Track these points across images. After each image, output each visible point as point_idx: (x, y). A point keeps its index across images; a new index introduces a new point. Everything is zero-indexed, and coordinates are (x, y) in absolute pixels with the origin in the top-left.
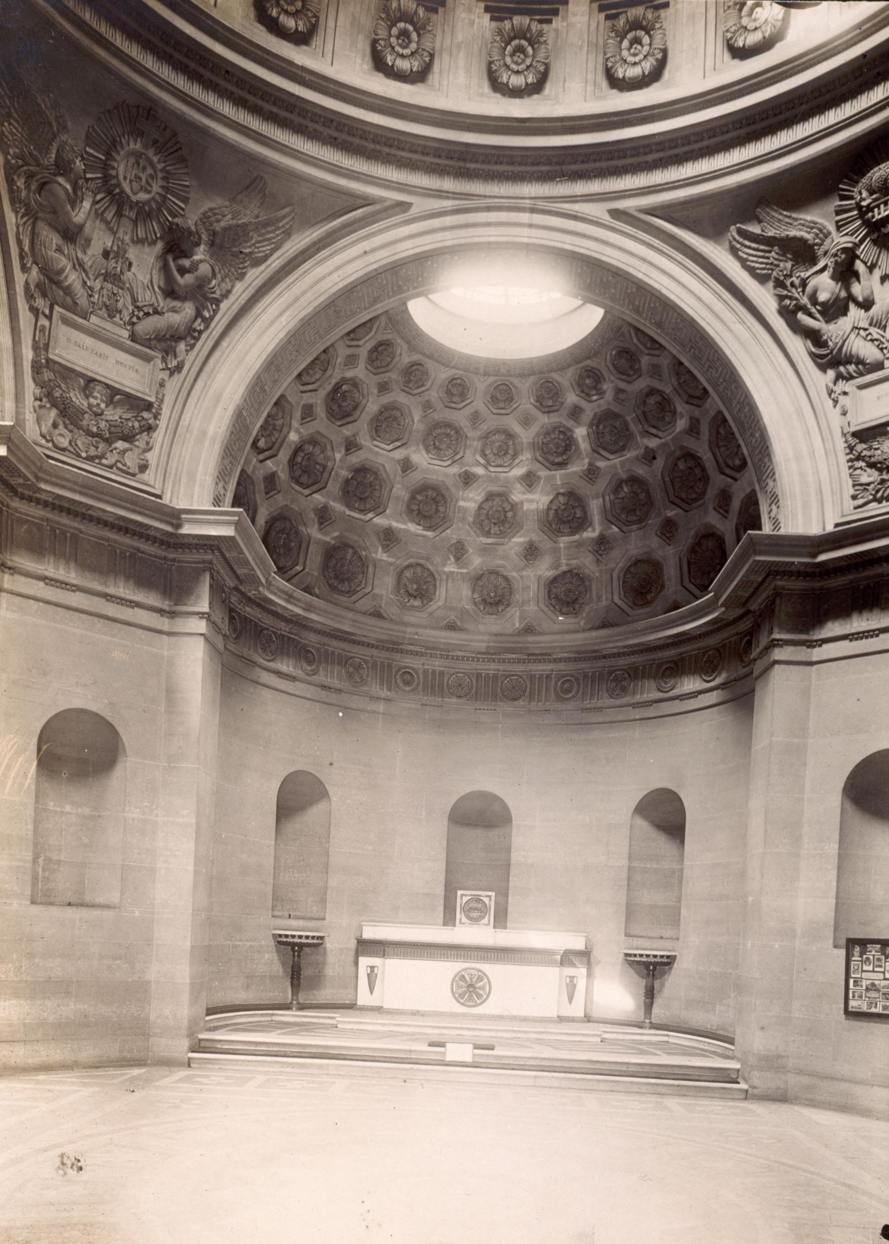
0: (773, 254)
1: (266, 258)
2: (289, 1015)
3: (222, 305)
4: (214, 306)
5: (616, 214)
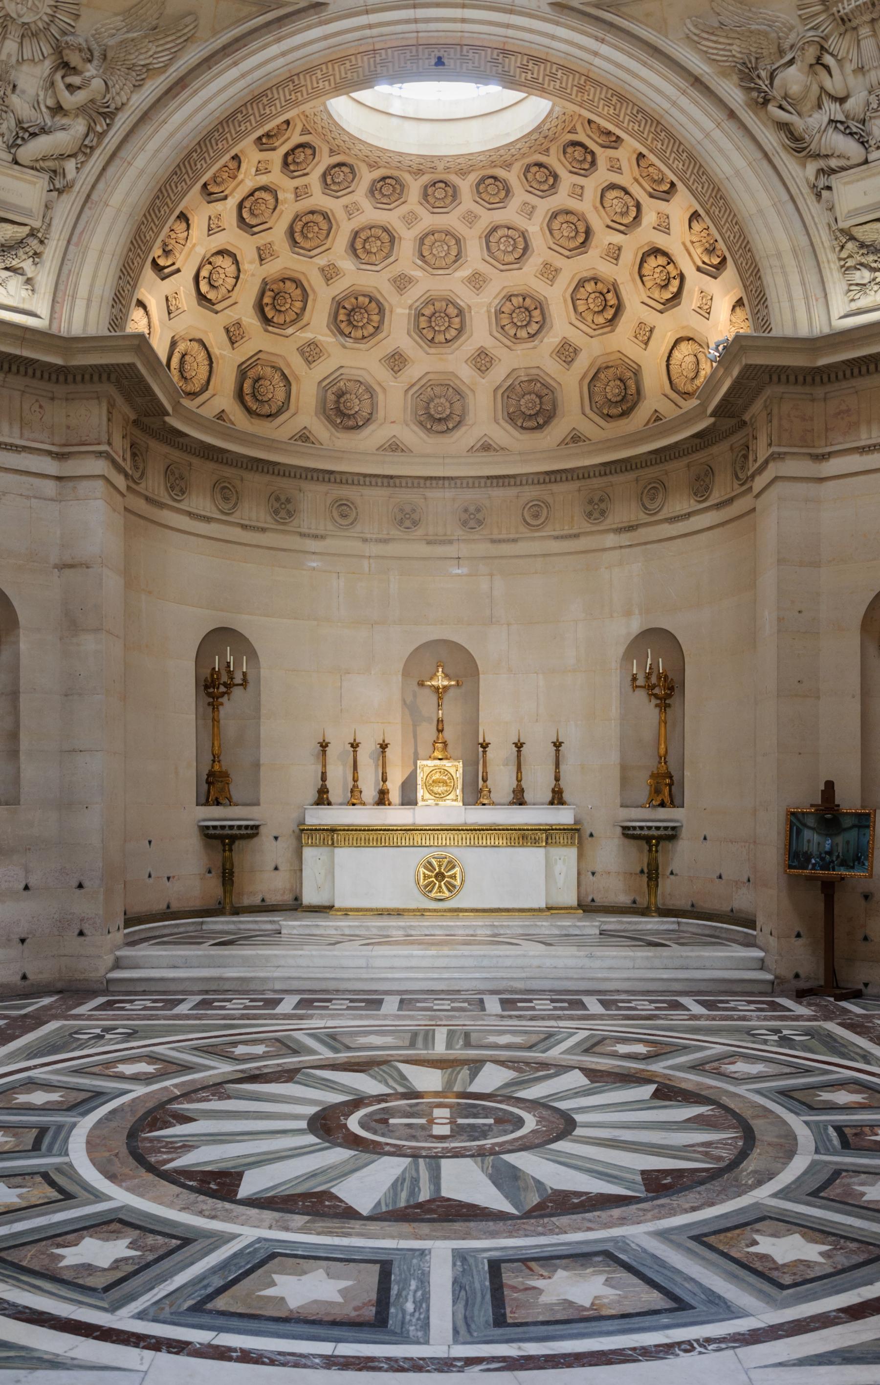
0: (734, 47)
1: (166, 67)
3: (116, 119)
4: (108, 121)
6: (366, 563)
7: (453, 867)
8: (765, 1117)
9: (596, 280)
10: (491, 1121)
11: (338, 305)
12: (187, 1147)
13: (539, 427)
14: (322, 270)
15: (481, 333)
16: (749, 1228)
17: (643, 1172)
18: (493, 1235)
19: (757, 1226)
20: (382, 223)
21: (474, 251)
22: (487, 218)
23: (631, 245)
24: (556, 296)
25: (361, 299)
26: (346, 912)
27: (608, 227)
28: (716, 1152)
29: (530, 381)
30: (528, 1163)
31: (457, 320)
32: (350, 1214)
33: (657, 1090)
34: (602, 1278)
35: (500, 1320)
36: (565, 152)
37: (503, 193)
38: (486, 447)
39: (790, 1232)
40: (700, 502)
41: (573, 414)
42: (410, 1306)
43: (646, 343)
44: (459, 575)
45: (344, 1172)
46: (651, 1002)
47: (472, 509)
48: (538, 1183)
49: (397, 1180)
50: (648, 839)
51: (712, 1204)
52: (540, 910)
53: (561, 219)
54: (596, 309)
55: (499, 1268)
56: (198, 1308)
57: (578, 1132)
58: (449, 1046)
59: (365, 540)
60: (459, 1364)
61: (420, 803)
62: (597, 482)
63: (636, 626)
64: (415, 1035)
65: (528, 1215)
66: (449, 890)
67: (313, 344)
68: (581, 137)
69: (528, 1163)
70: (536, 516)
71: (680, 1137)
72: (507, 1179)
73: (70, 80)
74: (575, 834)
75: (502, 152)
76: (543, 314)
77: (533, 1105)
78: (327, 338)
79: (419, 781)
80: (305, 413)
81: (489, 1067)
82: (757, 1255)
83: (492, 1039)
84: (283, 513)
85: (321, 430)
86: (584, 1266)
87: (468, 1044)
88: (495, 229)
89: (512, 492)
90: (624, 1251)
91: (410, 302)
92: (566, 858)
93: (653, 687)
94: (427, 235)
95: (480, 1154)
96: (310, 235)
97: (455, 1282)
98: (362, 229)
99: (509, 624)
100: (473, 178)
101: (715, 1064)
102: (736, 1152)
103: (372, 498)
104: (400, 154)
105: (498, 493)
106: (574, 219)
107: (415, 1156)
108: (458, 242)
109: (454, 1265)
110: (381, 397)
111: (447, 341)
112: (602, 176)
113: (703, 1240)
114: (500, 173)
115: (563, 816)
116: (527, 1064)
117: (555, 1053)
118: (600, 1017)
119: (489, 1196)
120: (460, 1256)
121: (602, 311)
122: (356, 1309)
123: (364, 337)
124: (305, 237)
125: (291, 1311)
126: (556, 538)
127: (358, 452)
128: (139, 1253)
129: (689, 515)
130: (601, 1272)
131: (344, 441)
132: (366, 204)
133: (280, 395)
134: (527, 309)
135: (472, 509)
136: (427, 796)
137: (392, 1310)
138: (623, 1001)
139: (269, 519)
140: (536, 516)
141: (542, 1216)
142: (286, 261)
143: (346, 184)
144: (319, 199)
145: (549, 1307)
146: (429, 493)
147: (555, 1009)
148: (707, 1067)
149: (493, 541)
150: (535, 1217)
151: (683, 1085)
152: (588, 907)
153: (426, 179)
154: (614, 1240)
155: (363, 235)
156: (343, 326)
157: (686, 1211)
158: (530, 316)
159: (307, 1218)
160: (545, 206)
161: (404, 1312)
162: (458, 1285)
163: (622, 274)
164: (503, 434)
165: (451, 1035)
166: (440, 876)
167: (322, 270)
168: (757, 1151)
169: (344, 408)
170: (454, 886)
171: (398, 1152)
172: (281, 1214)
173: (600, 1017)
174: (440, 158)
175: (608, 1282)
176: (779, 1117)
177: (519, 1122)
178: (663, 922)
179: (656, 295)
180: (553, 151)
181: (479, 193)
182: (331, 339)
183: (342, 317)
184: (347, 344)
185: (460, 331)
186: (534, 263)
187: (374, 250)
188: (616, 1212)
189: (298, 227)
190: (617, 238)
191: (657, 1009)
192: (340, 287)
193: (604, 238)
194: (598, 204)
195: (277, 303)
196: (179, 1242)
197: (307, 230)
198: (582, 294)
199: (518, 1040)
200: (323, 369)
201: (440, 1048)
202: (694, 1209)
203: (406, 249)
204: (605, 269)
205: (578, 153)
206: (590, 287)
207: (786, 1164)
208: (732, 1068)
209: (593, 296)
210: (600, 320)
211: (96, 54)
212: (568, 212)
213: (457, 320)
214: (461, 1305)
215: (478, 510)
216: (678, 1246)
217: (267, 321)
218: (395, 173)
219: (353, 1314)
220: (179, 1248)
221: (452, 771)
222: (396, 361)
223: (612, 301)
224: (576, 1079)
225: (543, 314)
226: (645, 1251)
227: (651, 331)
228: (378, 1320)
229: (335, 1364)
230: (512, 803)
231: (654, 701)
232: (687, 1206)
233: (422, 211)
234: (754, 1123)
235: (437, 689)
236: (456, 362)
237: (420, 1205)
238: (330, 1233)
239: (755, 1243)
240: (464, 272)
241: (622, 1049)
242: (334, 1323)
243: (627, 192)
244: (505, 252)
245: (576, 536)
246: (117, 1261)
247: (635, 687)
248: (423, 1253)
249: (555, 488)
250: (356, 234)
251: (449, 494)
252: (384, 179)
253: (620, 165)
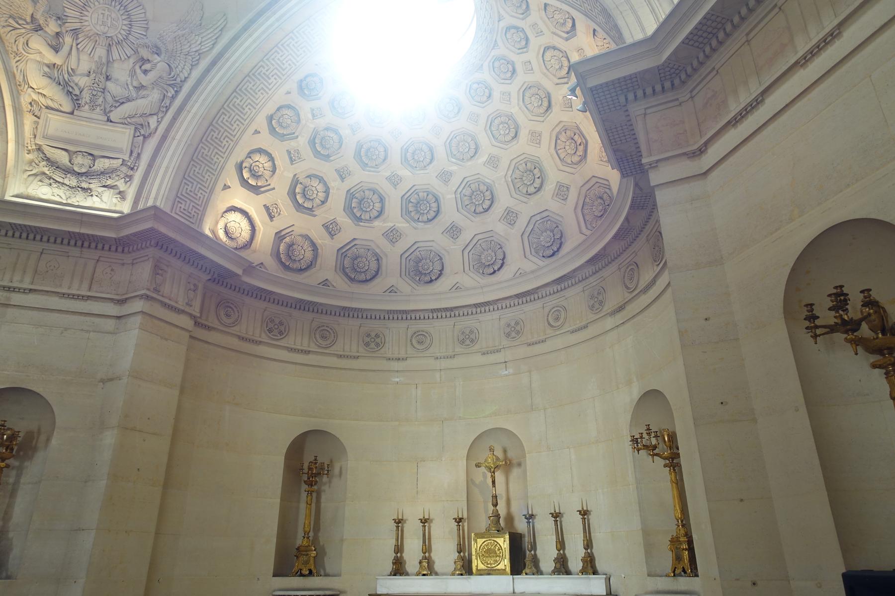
73: (145, 67)
80: (391, 276)
84: (373, 345)
85: (405, 286)
89: (538, 304)
91: (454, 189)
103: (441, 329)
139: (361, 349)
146: (482, 317)
211: (163, 49)
215: (517, 323)
222: (454, 231)
245: (585, 327)
251: (496, 315)
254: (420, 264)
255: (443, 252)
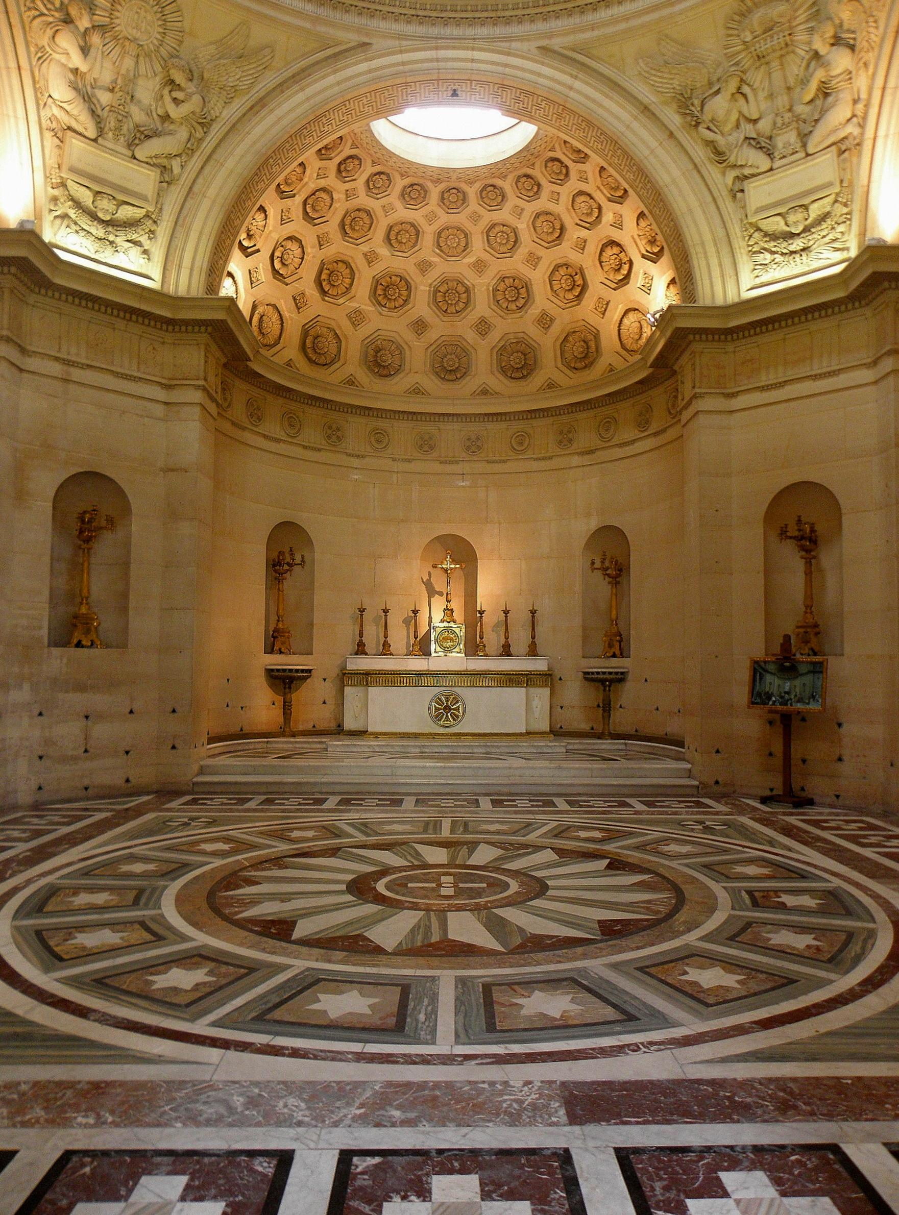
2: (283, 743)
5: (544, 49)
6: (395, 476)
7: (457, 702)
8: (692, 883)
9: (567, 265)
10: (485, 885)
11: (377, 282)
12: (255, 901)
13: (524, 377)
14: (365, 255)
15: (482, 306)
16: (680, 962)
17: (599, 922)
18: (485, 966)
19: (686, 961)
20: (411, 221)
21: (478, 243)
22: (488, 217)
23: (595, 237)
24: (538, 277)
25: (393, 278)
26: (376, 735)
27: (577, 224)
28: (654, 907)
29: (518, 342)
30: (511, 914)
31: (464, 296)
32: (378, 950)
33: (609, 863)
34: (570, 997)
35: (491, 1027)
36: (546, 167)
37: (500, 198)
38: (485, 392)
39: (712, 966)
40: (642, 431)
41: (550, 367)
42: (422, 1017)
43: (604, 314)
44: (463, 487)
45: (375, 920)
46: (605, 801)
47: (473, 438)
48: (521, 930)
49: (414, 927)
50: (602, 681)
51: (653, 945)
52: (521, 734)
53: (542, 218)
54: (567, 288)
55: (491, 990)
56: (260, 1018)
57: (550, 892)
58: (452, 832)
59: (394, 460)
60: (459, 1059)
61: (433, 654)
62: (565, 418)
63: (594, 524)
64: (427, 824)
65: (512, 952)
66: (454, 720)
67: (358, 312)
68: (558, 154)
69: (511, 914)
70: (520, 444)
71: (626, 897)
72: (497, 926)
74: (547, 678)
75: (499, 166)
76: (527, 291)
77: (515, 874)
78: (368, 308)
79: (433, 638)
80: (352, 364)
81: (482, 847)
82: (687, 981)
83: (485, 827)
85: (363, 376)
86: (556, 989)
87: (466, 830)
88: (493, 226)
89: (504, 425)
90: (586, 978)
91: (430, 281)
92: (541, 696)
93: (607, 569)
94: (444, 229)
95: (477, 908)
96: (357, 228)
97: (457, 999)
98: (396, 224)
99: (500, 524)
100: (478, 186)
101: (654, 846)
102: (670, 908)
104: (425, 166)
105: (493, 427)
106: (551, 218)
107: (428, 909)
108: (466, 235)
109: (456, 987)
110: (407, 352)
111: (457, 312)
112: (574, 185)
113: (645, 970)
114: (499, 182)
115: (540, 665)
116: (511, 844)
117: (532, 837)
118: (567, 812)
119: (484, 939)
120: (462, 982)
121: (571, 290)
122: (381, 1019)
123: (396, 308)
124: (353, 229)
125: (332, 1021)
126: (536, 459)
127: (389, 394)
128: (215, 979)
129: (633, 442)
130: (568, 993)
131: (379, 385)
132: (398, 205)
133: (333, 349)
134: (516, 288)
135: (473, 438)
136: (438, 649)
137: (408, 1020)
138: (584, 801)
140: (521, 444)
141: (523, 953)
142: (338, 247)
143: (384, 189)
144: (363, 200)
145: (529, 1018)
147: (533, 806)
148: (648, 847)
149: (488, 462)
150: (518, 953)
151: (629, 860)
152: (557, 732)
153: (442, 186)
154: (578, 970)
155: (396, 229)
156: (380, 298)
157: (633, 949)
158: (518, 293)
159: (345, 953)
160: (531, 208)
161: (417, 1021)
162: (459, 1002)
163: (587, 260)
164: (497, 382)
165: (454, 823)
166: (447, 708)
167: (365, 255)
168: (686, 908)
169: (381, 360)
170: (458, 717)
171: (415, 907)
172: (325, 951)
173: (567, 812)
174: (454, 170)
175: (573, 1001)
176: (702, 883)
177: (507, 886)
178: (614, 744)
179: (611, 277)
180: (537, 166)
181: (482, 198)
182: (372, 309)
183: (379, 292)
184: (384, 313)
185: (467, 304)
186: (522, 252)
187: (404, 241)
188: (579, 950)
189: (347, 222)
190: (584, 233)
191: (609, 806)
192: (379, 268)
193: (575, 233)
194: (570, 207)
195: (332, 279)
196: (246, 971)
197: (354, 224)
198: (557, 276)
199: (505, 827)
200: (365, 331)
201: (445, 833)
202: (638, 948)
203: (428, 240)
204: (574, 257)
205: (556, 167)
206: (562, 271)
207: (709, 917)
208: (666, 848)
209: (565, 277)
210: (570, 296)
212: (548, 213)
213: (464, 296)
214: (461, 1018)
216: (627, 974)
217: (324, 292)
218: (421, 181)
219: (379, 1022)
220: (246, 975)
221: (457, 631)
223: (580, 282)
224: (548, 856)
225: (527, 291)
226: (601, 978)
227: (607, 304)
228: (398, 1026)
229: (364, 1059)
230: (501, 655)
231: (608, 579)
232: (634, 945)
233: (440, 212)
234: (683, 887)
235: (446, 570)
236: (464, 328)
237: (431, 945)
238: (364, 965)
239: (686, 973)
240: (470, 259)
241: (583, 834)
242: (364, 1029)
243: (592, 198)
244: (501, 244)
245: (550, 458)
246: (197, 985)
247: (593, 569)
248: (433, 979)
249: (535, 423)
250: (391, 228)
251: (457, 426)
252: (412, 185)
253: (587, 177)
254: (379, 355)
255: (403, 345)
